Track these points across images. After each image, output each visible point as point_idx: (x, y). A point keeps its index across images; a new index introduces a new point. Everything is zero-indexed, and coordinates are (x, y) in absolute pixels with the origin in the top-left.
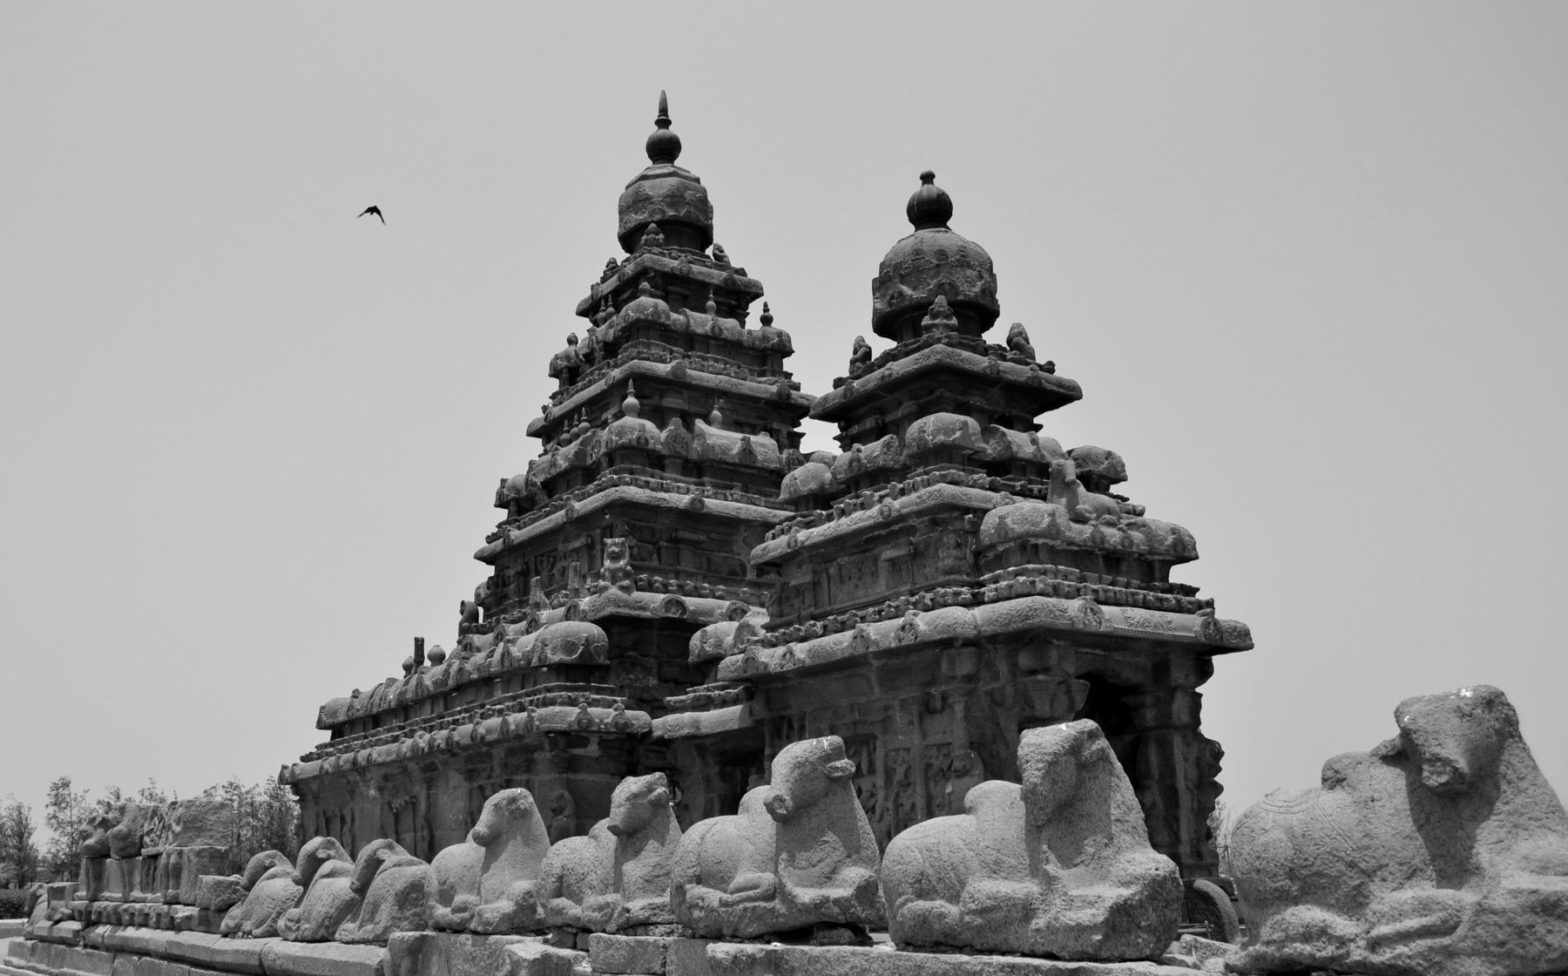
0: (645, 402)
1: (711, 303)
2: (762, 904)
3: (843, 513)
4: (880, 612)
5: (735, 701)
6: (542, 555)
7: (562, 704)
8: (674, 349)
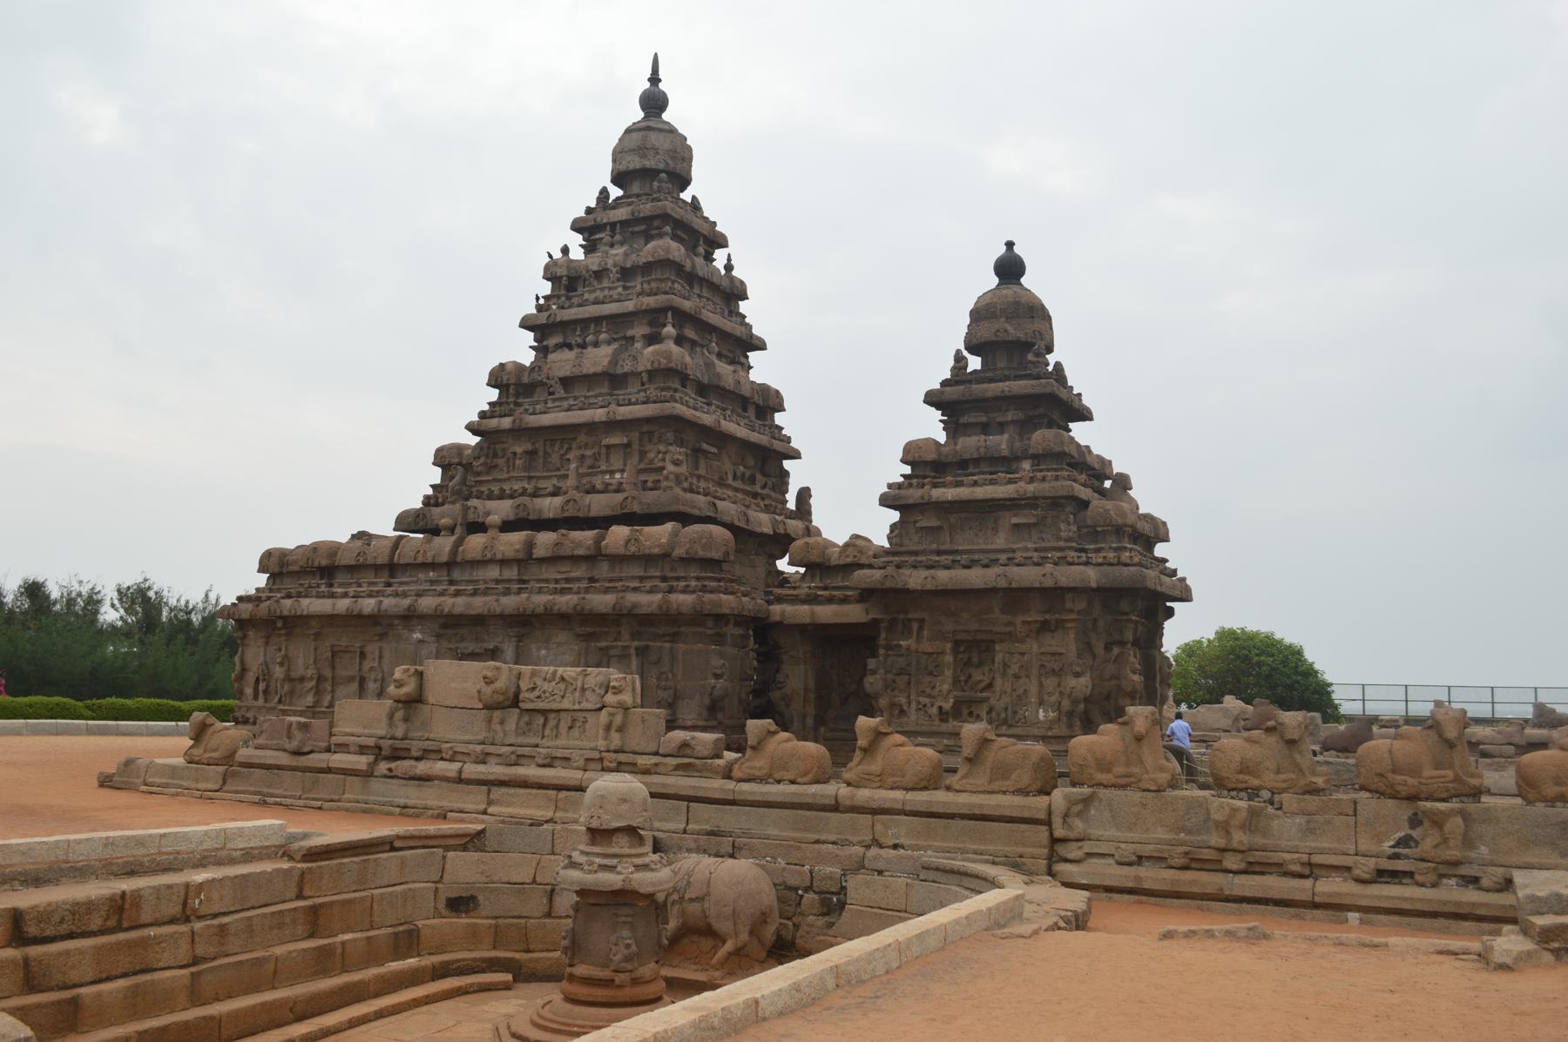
1: (701, 250)
2: (1450, 785)
3: (975, 483)
4: (1009, 559)
5: (844, 601)
6: (552, 440)
7: (720, 592)
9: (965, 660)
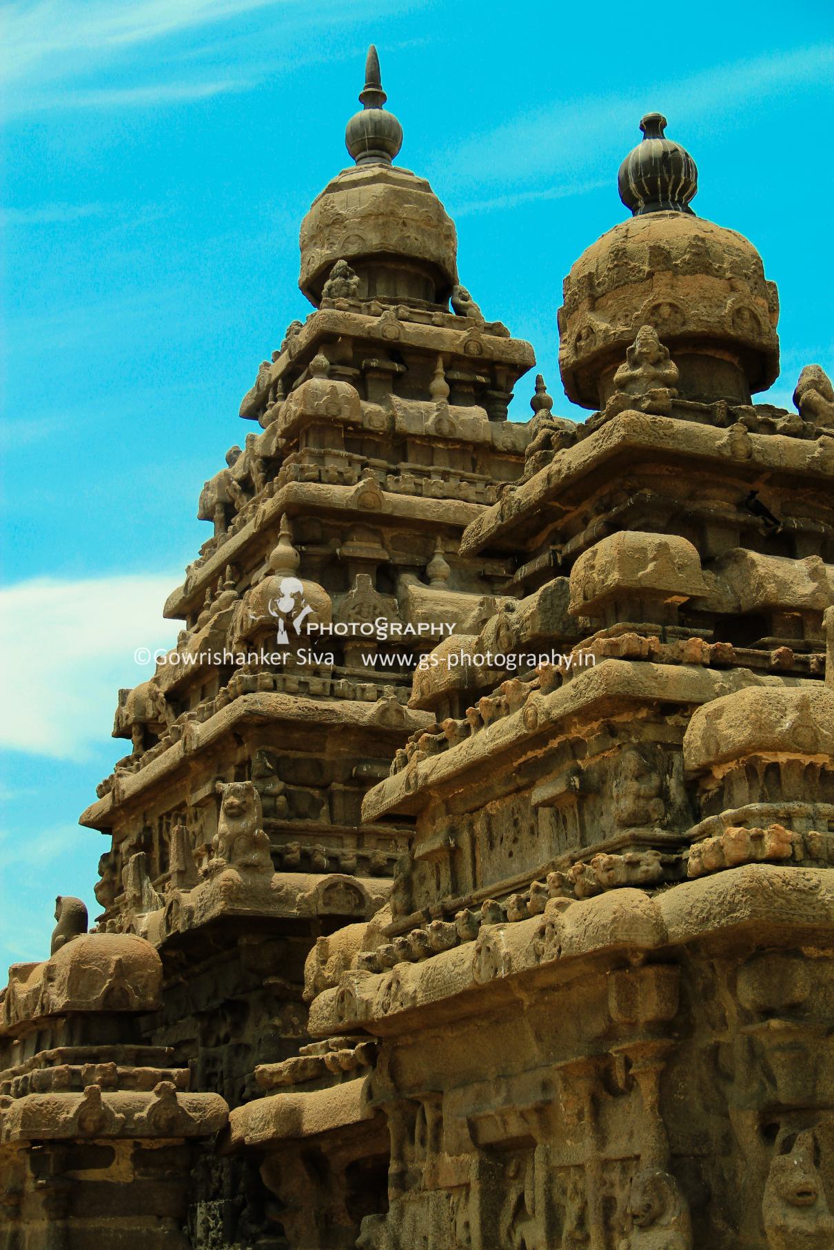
0: (312, 550)
1: (439, 384)
5: (358, 1071)
6: (168, 815)
8: (373, 461)
9: (513, 1197)
